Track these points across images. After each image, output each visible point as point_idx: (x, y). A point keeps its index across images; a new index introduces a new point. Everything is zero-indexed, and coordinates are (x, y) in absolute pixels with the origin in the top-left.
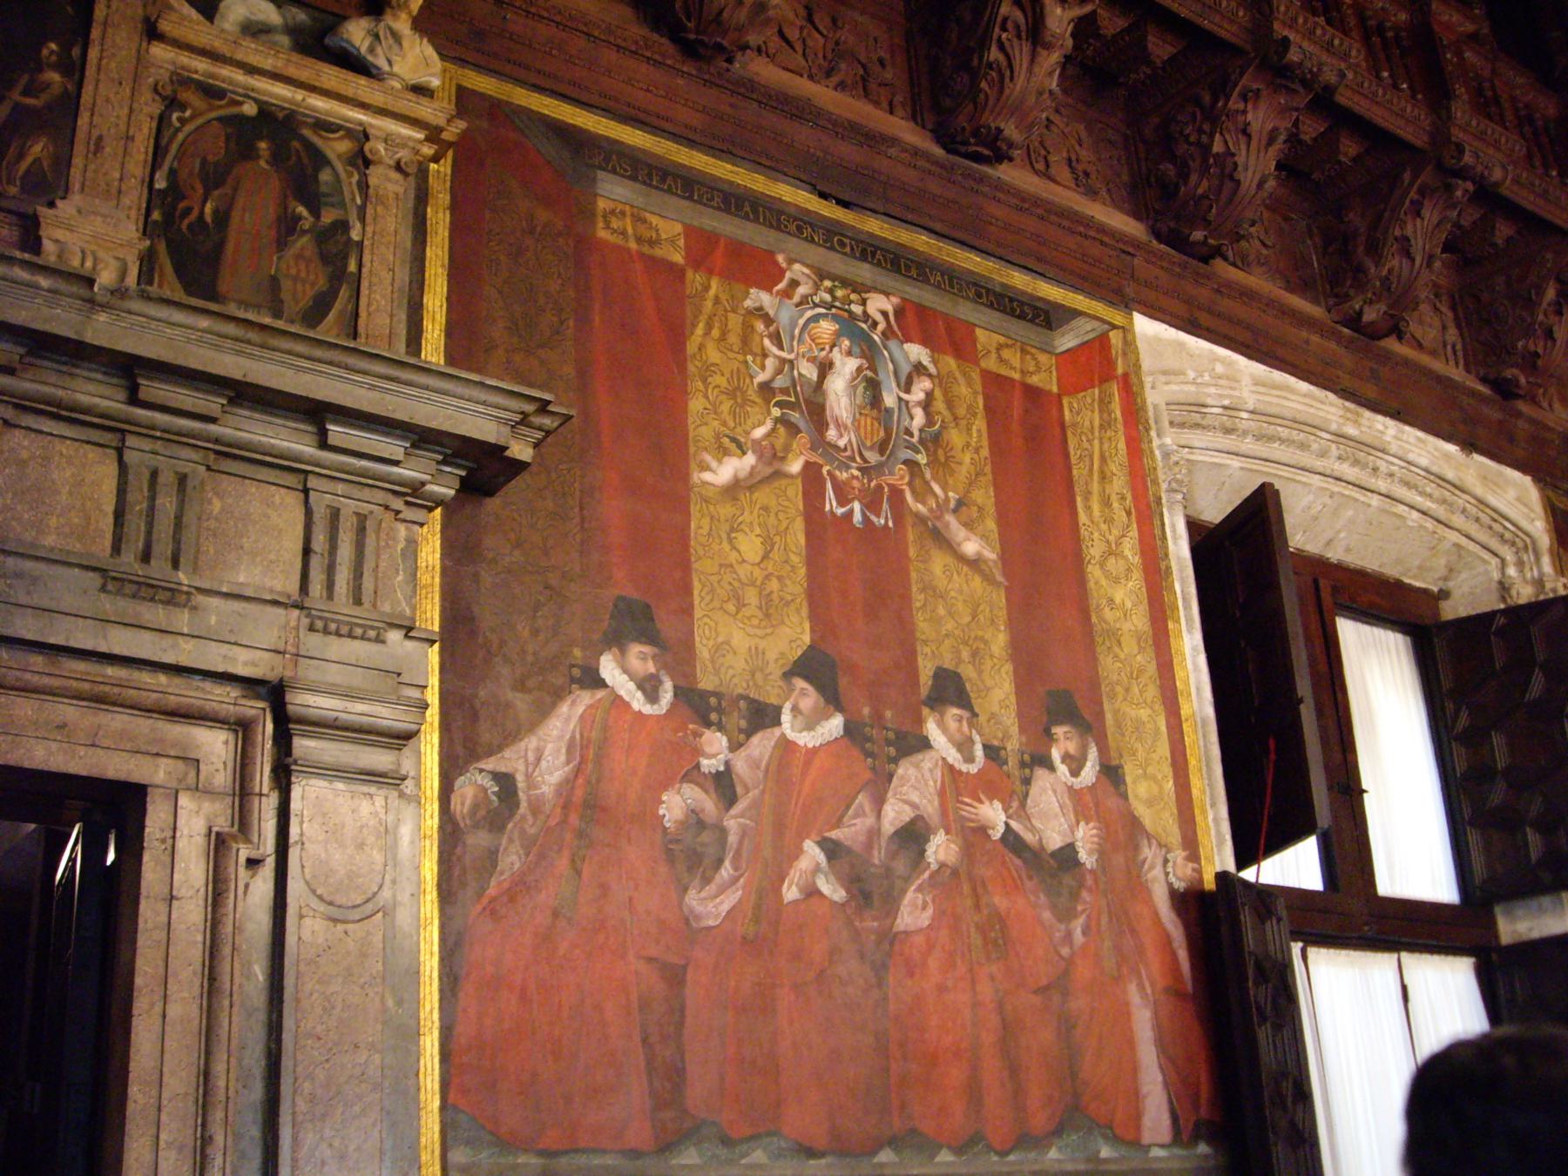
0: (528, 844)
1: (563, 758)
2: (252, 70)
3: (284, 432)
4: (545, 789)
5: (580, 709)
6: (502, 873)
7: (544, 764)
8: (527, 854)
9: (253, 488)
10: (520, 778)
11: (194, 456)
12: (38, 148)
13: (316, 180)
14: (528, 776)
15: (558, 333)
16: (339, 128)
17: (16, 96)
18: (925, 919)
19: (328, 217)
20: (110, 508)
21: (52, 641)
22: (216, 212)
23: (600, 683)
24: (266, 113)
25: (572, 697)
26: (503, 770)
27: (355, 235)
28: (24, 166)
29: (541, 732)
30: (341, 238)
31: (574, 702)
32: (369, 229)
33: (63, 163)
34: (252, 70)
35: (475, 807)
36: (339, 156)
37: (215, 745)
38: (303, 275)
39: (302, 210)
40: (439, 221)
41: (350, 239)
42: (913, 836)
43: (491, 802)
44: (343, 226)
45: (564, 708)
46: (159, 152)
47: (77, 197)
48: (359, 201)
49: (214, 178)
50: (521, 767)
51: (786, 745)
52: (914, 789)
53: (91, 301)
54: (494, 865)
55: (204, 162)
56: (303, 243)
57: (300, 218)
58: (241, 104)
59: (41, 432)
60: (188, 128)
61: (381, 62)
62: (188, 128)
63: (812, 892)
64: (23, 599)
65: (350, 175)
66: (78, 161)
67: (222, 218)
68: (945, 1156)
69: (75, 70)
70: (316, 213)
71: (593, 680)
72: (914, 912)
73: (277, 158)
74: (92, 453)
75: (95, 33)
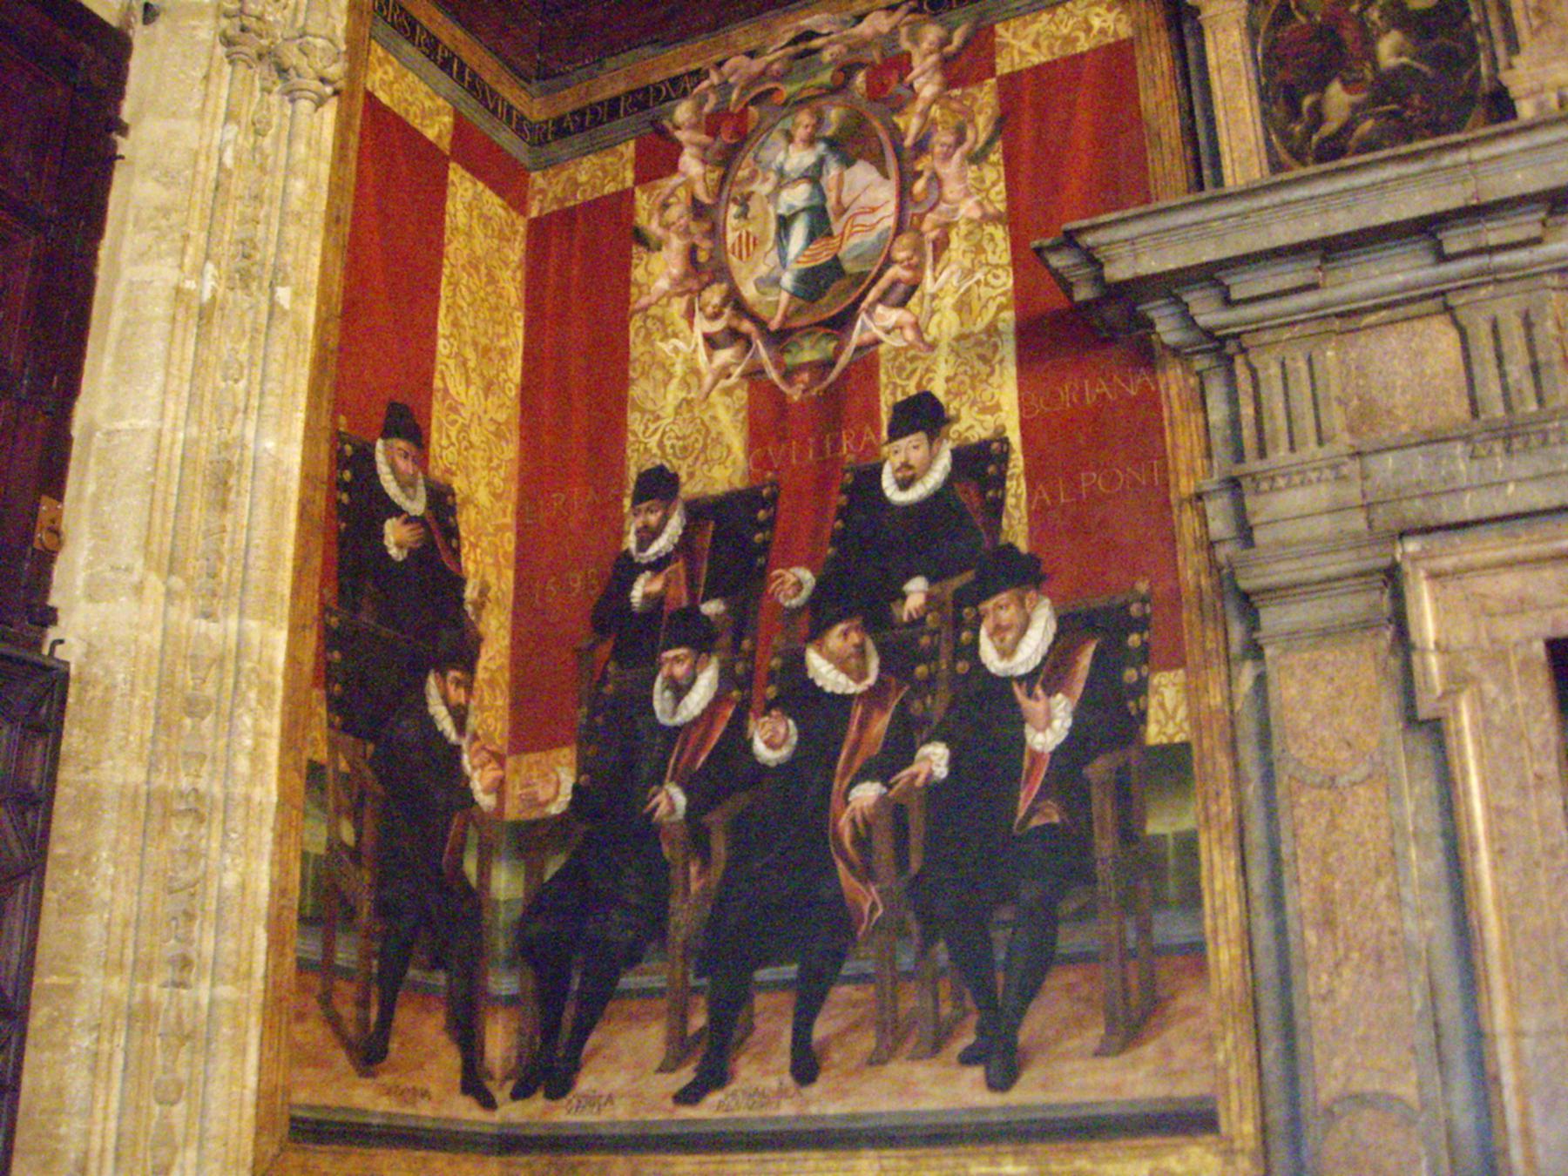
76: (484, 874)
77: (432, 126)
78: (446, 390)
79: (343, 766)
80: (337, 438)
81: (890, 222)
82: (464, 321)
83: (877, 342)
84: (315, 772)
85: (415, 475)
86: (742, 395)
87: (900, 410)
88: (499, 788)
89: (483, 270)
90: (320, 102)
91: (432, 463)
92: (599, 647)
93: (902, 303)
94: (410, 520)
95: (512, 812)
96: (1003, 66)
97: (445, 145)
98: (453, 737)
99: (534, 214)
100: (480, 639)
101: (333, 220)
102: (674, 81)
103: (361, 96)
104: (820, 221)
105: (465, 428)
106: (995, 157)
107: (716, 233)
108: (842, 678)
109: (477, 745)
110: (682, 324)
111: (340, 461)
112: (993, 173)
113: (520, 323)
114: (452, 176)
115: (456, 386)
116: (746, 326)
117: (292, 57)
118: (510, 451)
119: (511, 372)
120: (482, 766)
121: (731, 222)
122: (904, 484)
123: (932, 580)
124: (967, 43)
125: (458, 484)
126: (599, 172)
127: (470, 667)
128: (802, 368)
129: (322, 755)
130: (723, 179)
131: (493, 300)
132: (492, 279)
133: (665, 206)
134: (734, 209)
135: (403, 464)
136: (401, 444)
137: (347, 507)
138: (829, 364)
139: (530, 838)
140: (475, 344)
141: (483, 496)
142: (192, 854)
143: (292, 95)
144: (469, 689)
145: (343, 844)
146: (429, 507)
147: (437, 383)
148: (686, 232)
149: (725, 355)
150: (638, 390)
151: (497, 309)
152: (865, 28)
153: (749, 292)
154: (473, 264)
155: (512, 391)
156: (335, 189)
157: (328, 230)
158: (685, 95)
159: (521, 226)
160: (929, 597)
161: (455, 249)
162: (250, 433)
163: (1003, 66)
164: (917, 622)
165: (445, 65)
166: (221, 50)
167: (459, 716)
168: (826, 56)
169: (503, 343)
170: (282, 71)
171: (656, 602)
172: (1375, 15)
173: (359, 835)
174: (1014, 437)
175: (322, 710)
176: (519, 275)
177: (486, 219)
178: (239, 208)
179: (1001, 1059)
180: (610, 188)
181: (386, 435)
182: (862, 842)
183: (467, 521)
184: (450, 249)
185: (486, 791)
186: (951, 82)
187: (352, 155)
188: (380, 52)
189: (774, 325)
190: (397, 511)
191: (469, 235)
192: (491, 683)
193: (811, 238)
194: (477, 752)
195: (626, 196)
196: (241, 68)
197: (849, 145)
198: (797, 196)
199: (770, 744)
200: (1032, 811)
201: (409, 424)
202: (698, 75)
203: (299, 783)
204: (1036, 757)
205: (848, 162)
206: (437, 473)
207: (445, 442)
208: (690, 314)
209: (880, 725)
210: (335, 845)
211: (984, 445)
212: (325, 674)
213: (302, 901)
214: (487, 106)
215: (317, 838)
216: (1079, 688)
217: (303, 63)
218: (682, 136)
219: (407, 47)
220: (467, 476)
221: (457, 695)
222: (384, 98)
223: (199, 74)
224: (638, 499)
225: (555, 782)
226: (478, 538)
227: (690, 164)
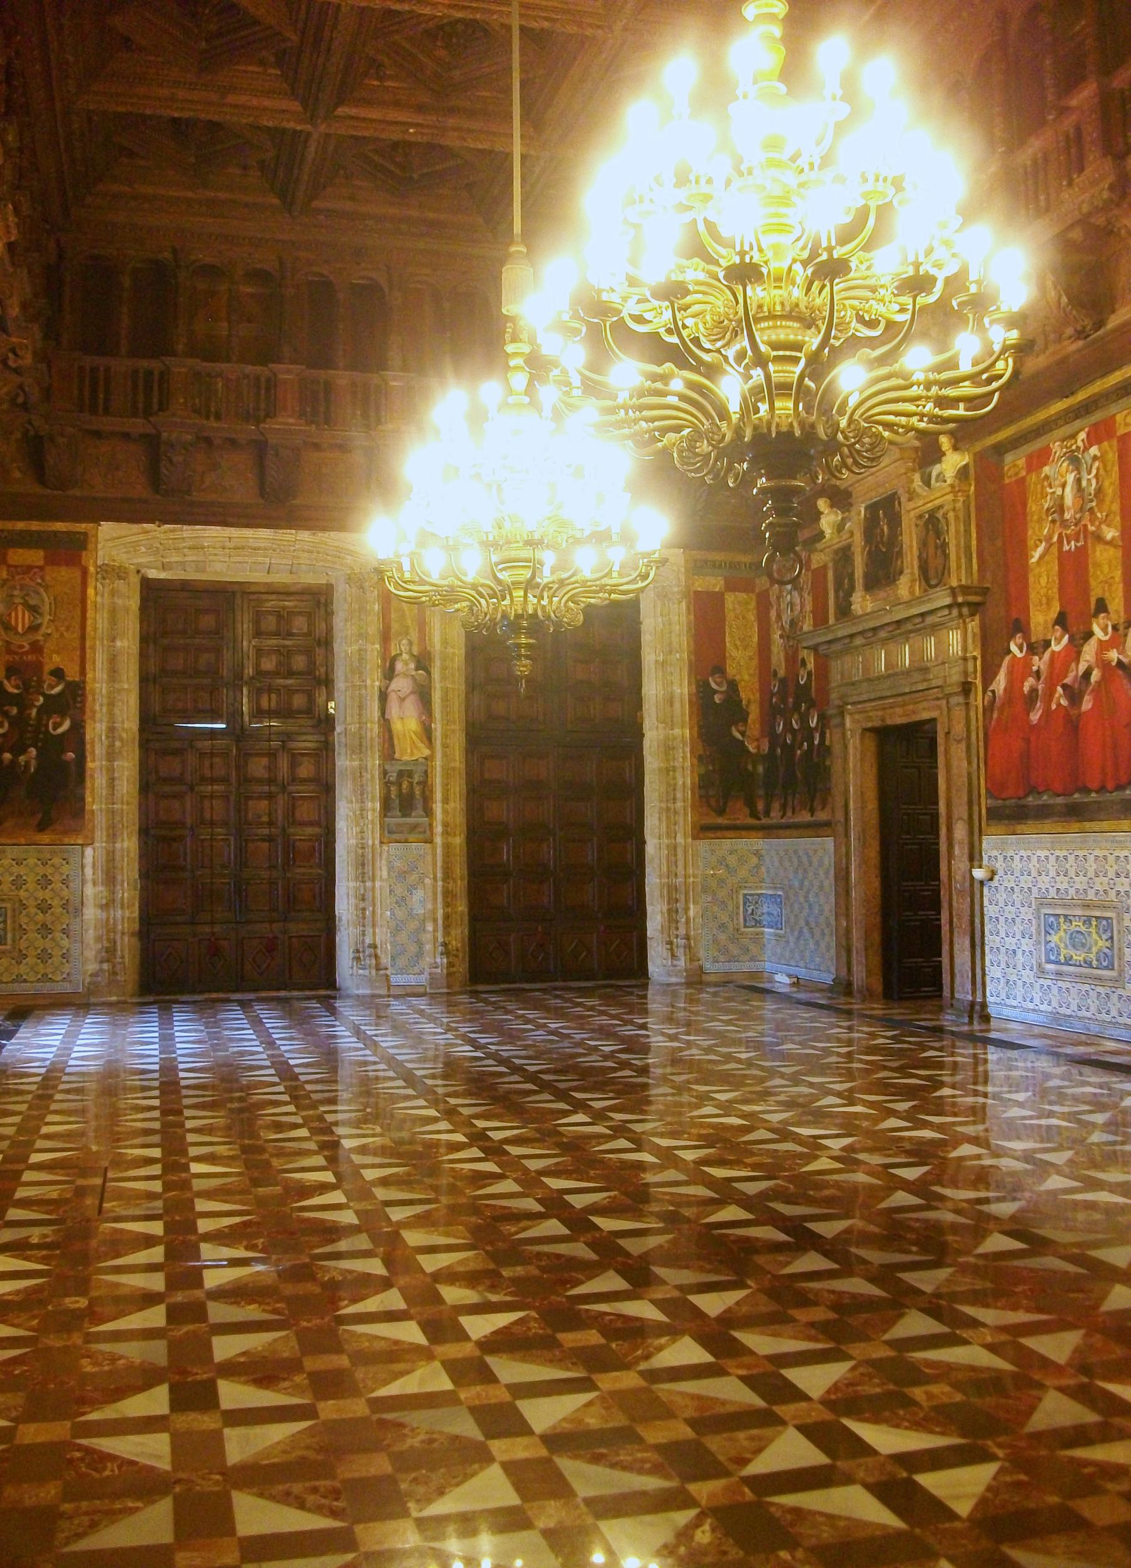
18: (1090, 706)
42: (1087, 674)
51: (1053, 652)
52: (1089, 652)
63: (1059, 705)
68: (1093, 795)
72: (1087, 704)
76: (755, 767)
80: (697, 682)
84: (700, 758)
88: (758, 747)
92: (771, 713)
111: (698, 686)
113: (756, 624)
115: (734, 653)
118: (755, 662)
125: (737, 678)
127: (745, 721)
137: (702, 698)
141: (746, 677)
142: (674, 778)
154: (737, 617)
155: (755, 645)
156: (689, 623)
167: (743, 734)
179: (812, 811)
181: (712, 674)
190: (716, 692)
201: (719, 669)
203: (695, 761)
206: (730, 677)
212: (700, 735)
215: (703, 770)
221: (742, 728)
225: (765, 747)
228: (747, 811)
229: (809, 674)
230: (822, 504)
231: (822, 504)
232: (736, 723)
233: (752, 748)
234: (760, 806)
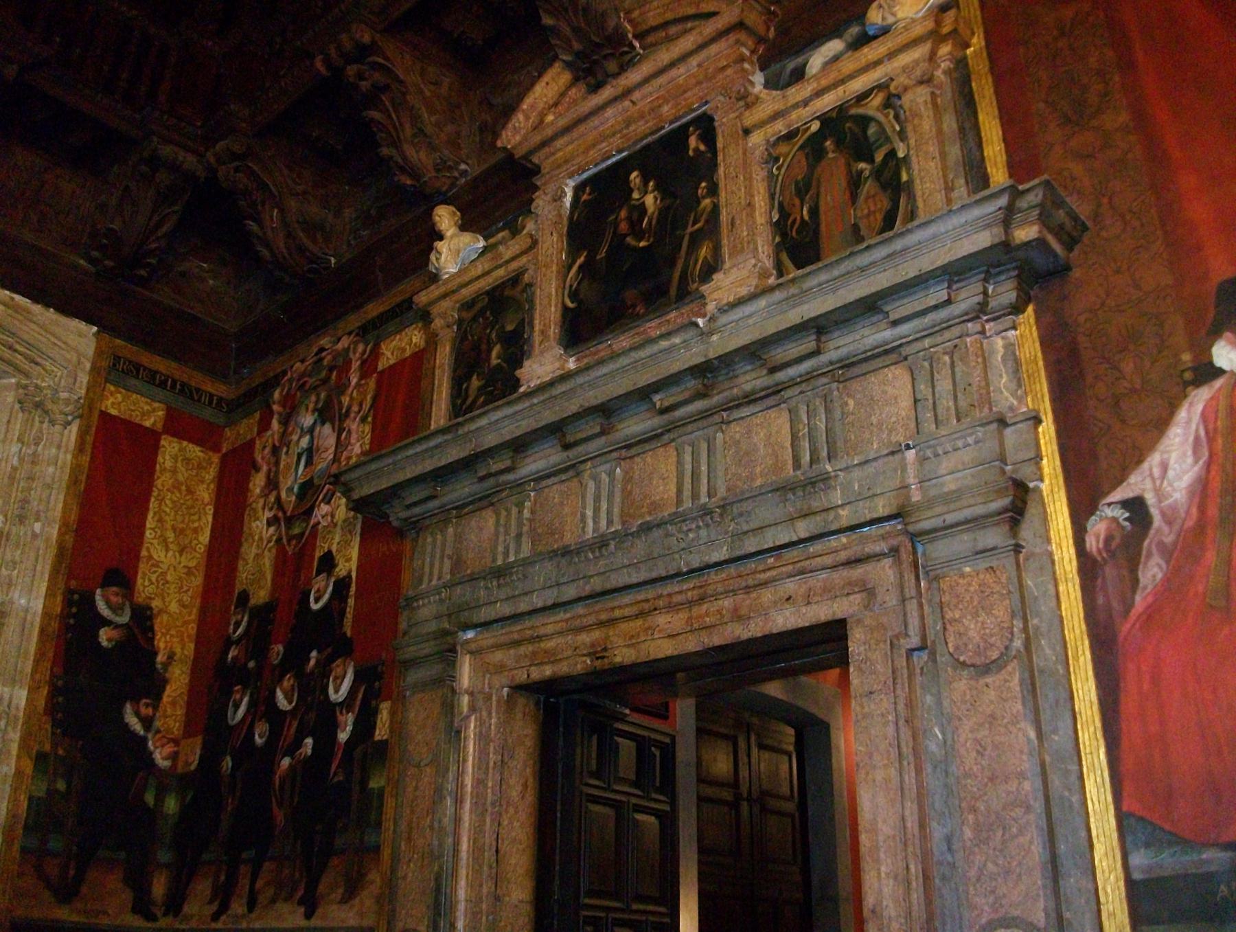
0: (1167, 552)
1: (1190, 460)
2: (805, 103)
3: (866, 332)
4: (1177, 496)
5: (1199, 408)
6: (1145, 588)
7: (1171, 473)
8: (1167, 562)
9: (872, 378)
10: (1150, 498)
11: (824, 380)
12: (704, 252)
13: (866, 138)
14: (1157, 491)
15: (1106, 95)
16: (872, 89)
17: (690, 230)
19: (879, 157)
20: (788, 444)
21: (766, 546)
22: (810, 212)
23: (1221, 372)
24: (825, 119)
25: (1189, 399)
26: (1131, 495)
27: (901, 154)
28: (698, 267)
29: (1161, 446)
30: (892, 164)
31: (1191, 404)
32: (912, 142)
33: (717, 249)
34: (805, 103)
35: (1109, 539)
36: (878, 109)
37: (884, 573)
38: (872, 209)
39: (862, 165)
40: (984, 90)
41: (898, 159)
43: (1123, 528)
44: (892, 153)
45: (1182, 414)
46: (772, 196)
47: (727, 266)
48: (898, 128)
49: (803, 188)
50: (1148, 484)
53: (702, 334)
54: (1135, 582)
55: (797, 183)
56: (869, 187)
57: (862, 171)
58: (809, 128)
59: (742, 418)
60: (783, 170)
61: (891, 20)
62: (783, 170)
64: (745, 528)
65: (887, 116)
66: (725, 242)
67: (814, 212)
69: (713, 190)
70: (871, 160)
71: (1207, 372)
73: (839, 144)
74: (773, 413)
75: (720, 158)
76: (159, 799)
77: (149, 418)
78: (150, 557)
79: (61, 752)
80: (69, 592)
81: (331, 457)
82: (167, 518)
83: (319, 523)
84: (41, 759)
85: (124, 604)
86: (274, 551)
87: (321, 558)
88: (174, 757)
89: (184, 488)
90: (69, 423)
91: (136, 595)
93: (328, 503)
94: (117, 626)
95: (180, 770)
96: (380, 368)
97: (159, 427)
98: (142, 733)
99: (224, 450)
100: (164, 682)
101: (73, 481)
102: (276, 377)
103: (96, 414)
104: (310, 452)
105: (164, 574)
106: (370, 419)
107: (277, 463)
108: (285, 702)
109: (158, 736)
110: (261, 513)
111: (68, 603)
112: (367, 428)
113: (210, 510)
114: (163, 442)
115: (159, 554)
116: (280, 514)
117: (49, 406)
118: (198, 581)
119: (201, 539)
120: (163, 746)
121: (283, 456)
122: (317, 600)
123: (319, 652)
124: (371, 352)
125: (156, 604)
126: (246, 428)
127: (158, 697)
128: (294, 537)
129: (47, 747)
130: (285, 431)
131: (189, 503)
132: (190, 491)
133: (265, 447)
134: (285, 450)
135: (114, 599)
136: (115, 589)
137: (72, 628)
138: (303, 534)
139: (185, 781)
140: (174, 529)
141: (174, 607)
143: (52, 422)
144: (156, 708)
145: (57, 791)
146: (131, 618)
147: (144, 553)
148: (268, 464)
149: (272, 529)
150: (244, 548)
151: (193, 507)
152: (340, 346)
153: (283, 495)
154: (177, 486)
156: (76, 469)
157: (68, 488)
158: (278, 385)
159: (216, 458)
160: (317, 661)
161: (162, 481)
162: (16, 595)
163: (380, 368)
164: (312, 673)
165: (162, 385)
166: (17, 406)
167: (147, 722)
168: (325, 362)
169: (196, 525)
170: (46, 412)
171: (235, 658)
172: (494, 335)
173: (69, 786)
174: (354, 575)
175: (48, 727)
176: (212, 486)
177: (187, 461)
178: (22, 484)
180: (249, 437)
181: (104, 585)
182: (282, 788)
183: (160, 623)
184: (159, 483)
185: (164, 759)
186: (361, 378)
187: (89, 448)
188: (112, 388)
189: (289, 514)
190: (106, 622)
191: (174, 471)
192: (173, 704)
193: (306, 467)
194: (160, 739)
195: (250, 445)
196: (26, 414)
197: (325, 414)
198: (304, 443)
199: (260, 737)
200: (335, 774)
201: (121, 577)
202: (284, 373)
204: (340, 744)
205: (323, 423)
206: (140, 599)
207: (147, 583)
208: (264, 509)
209: (295, 724)
210: (51, 793)
211: (344, 578)
213: (27, 818)
214: (192, 399)
215: (41, 790)
216: (357, 709)
217: (55, 408)
218: (275, 407)
219: (134, 381)
220: (163, 599)
221: (146, 711)
222: (114, 412)
223: (5, 420)
224: (236, 608)
225: (193, 753)
226: (169, 630)
227: (275, 424)
228: (127, 896)
229: (342, 586)
230: (445, 218)
231: (445, 218)
232: (135, 700)
233: (160, 758)
234: (159, 888)
